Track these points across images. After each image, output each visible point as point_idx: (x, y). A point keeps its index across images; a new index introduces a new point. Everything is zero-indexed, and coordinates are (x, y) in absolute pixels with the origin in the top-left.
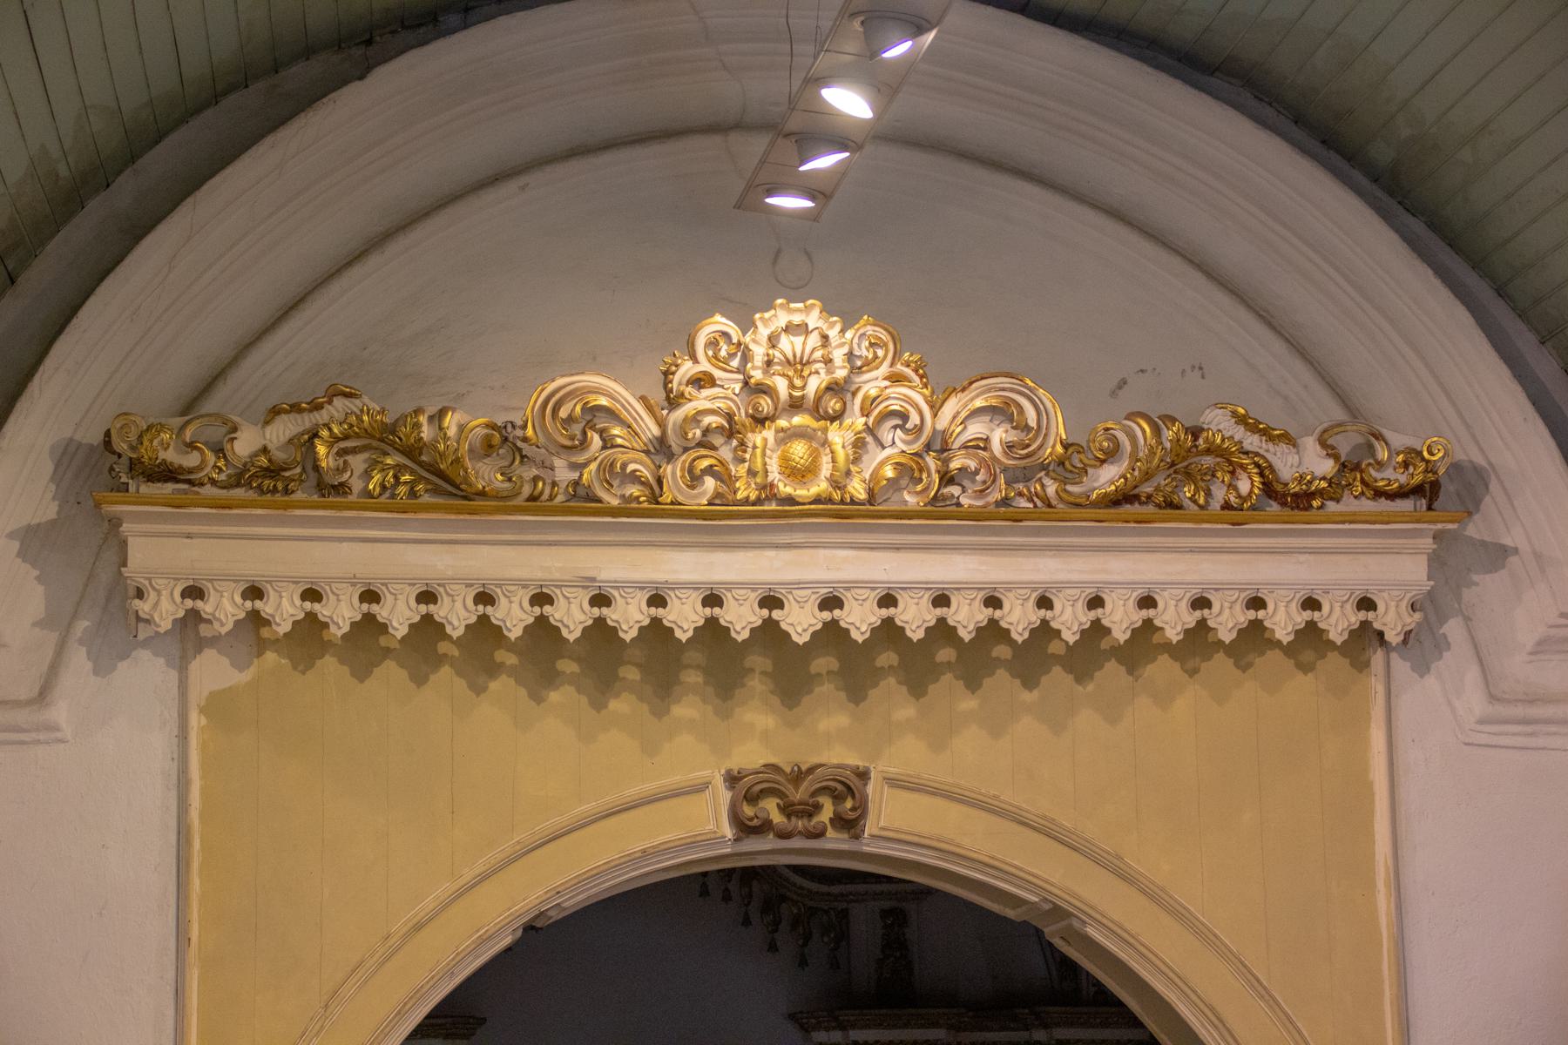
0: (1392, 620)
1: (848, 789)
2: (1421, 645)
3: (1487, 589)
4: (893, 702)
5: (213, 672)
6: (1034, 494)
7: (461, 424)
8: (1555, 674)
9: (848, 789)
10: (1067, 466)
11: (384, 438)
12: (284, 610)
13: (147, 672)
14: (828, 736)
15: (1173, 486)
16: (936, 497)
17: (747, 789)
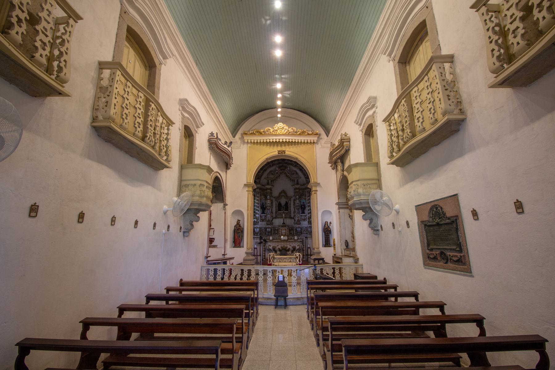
0: (315, 141)
1: (284, 151)
2: (317, 143)
3: (321, 141)
4: (287, 147)
5: (249, 145)
6: (294, 134)
7: (262, 130)
8: (325, 145)
9: (284, 151)
10: (296, 132)
11: (258, 132)
12: (253, 141)
13: (246, 145)
14: (283, 148)
15: (302, 133)
16: (288, 134)
17: (279, 151)
